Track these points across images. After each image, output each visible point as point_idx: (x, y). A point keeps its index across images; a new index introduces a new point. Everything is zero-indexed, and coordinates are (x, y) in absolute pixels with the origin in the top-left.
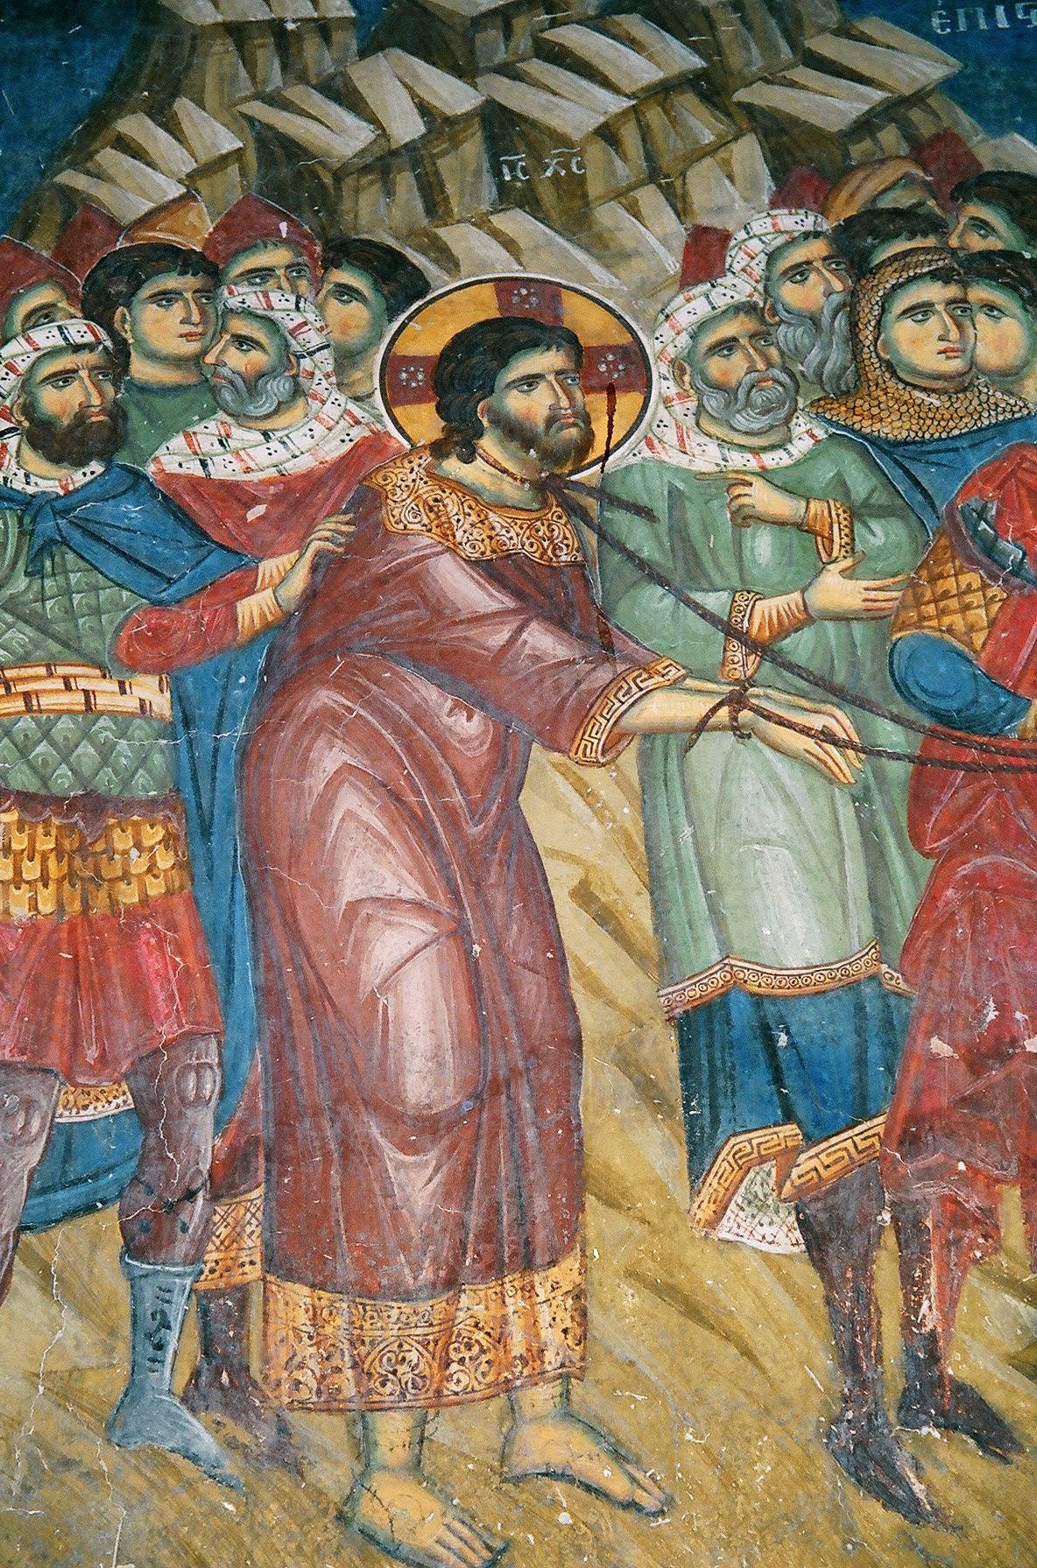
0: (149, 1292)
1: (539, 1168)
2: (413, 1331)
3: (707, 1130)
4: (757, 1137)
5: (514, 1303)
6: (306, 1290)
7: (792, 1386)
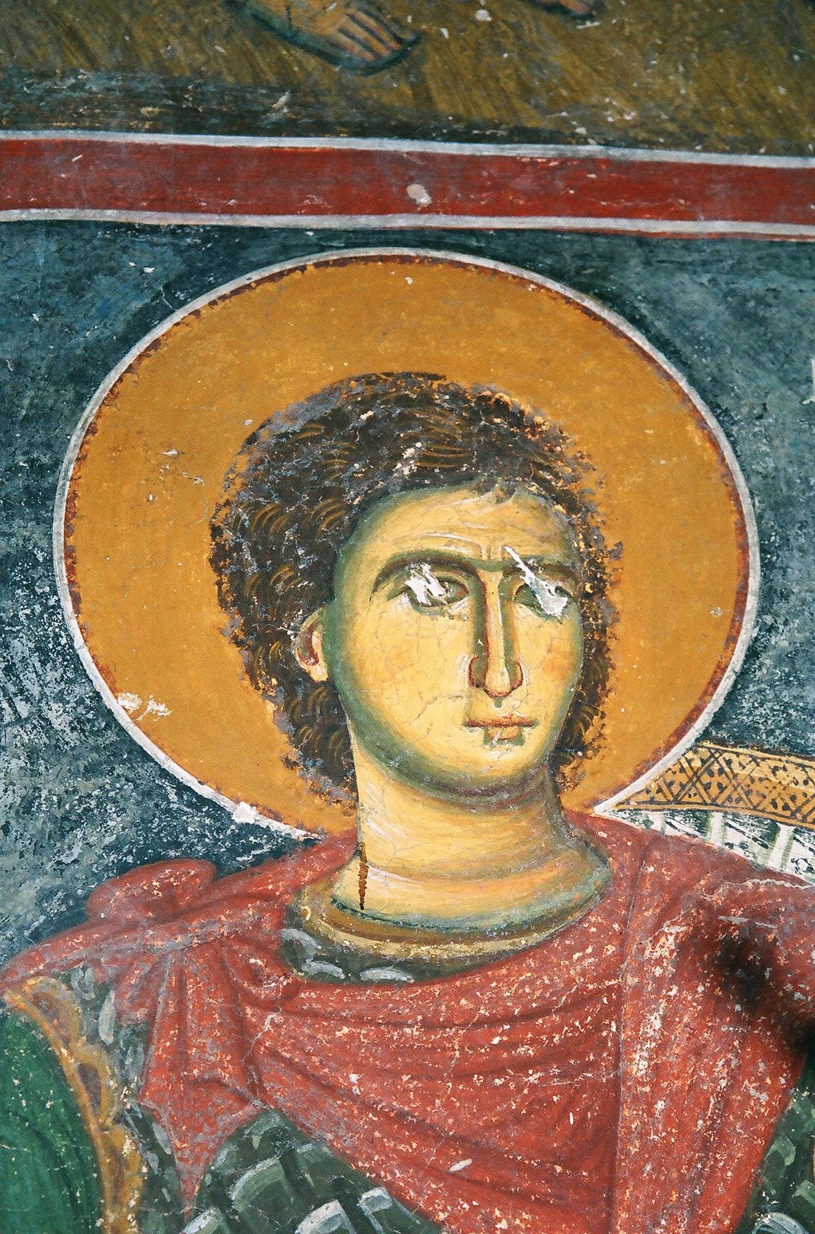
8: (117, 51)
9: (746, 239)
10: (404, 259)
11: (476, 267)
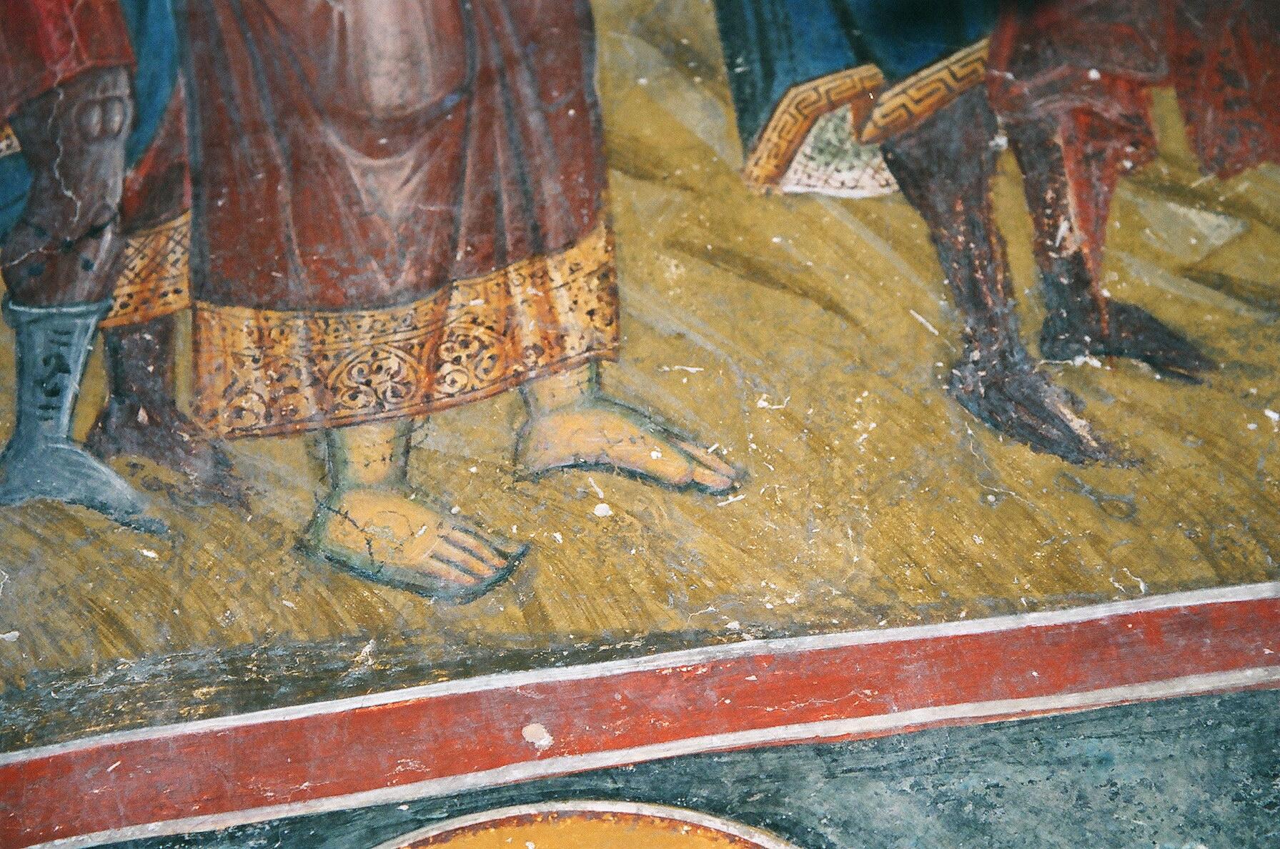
0: (40, 338)
1: (547, 153)
2: (391, 338)
3: (760, 85)
4: (824, 84)
5: (521, 292)
6: (248, 312)
7: (896, 333)
8: (166, 628)
9: (954, 727)
10: (521, 820)
11: (614, 814)
